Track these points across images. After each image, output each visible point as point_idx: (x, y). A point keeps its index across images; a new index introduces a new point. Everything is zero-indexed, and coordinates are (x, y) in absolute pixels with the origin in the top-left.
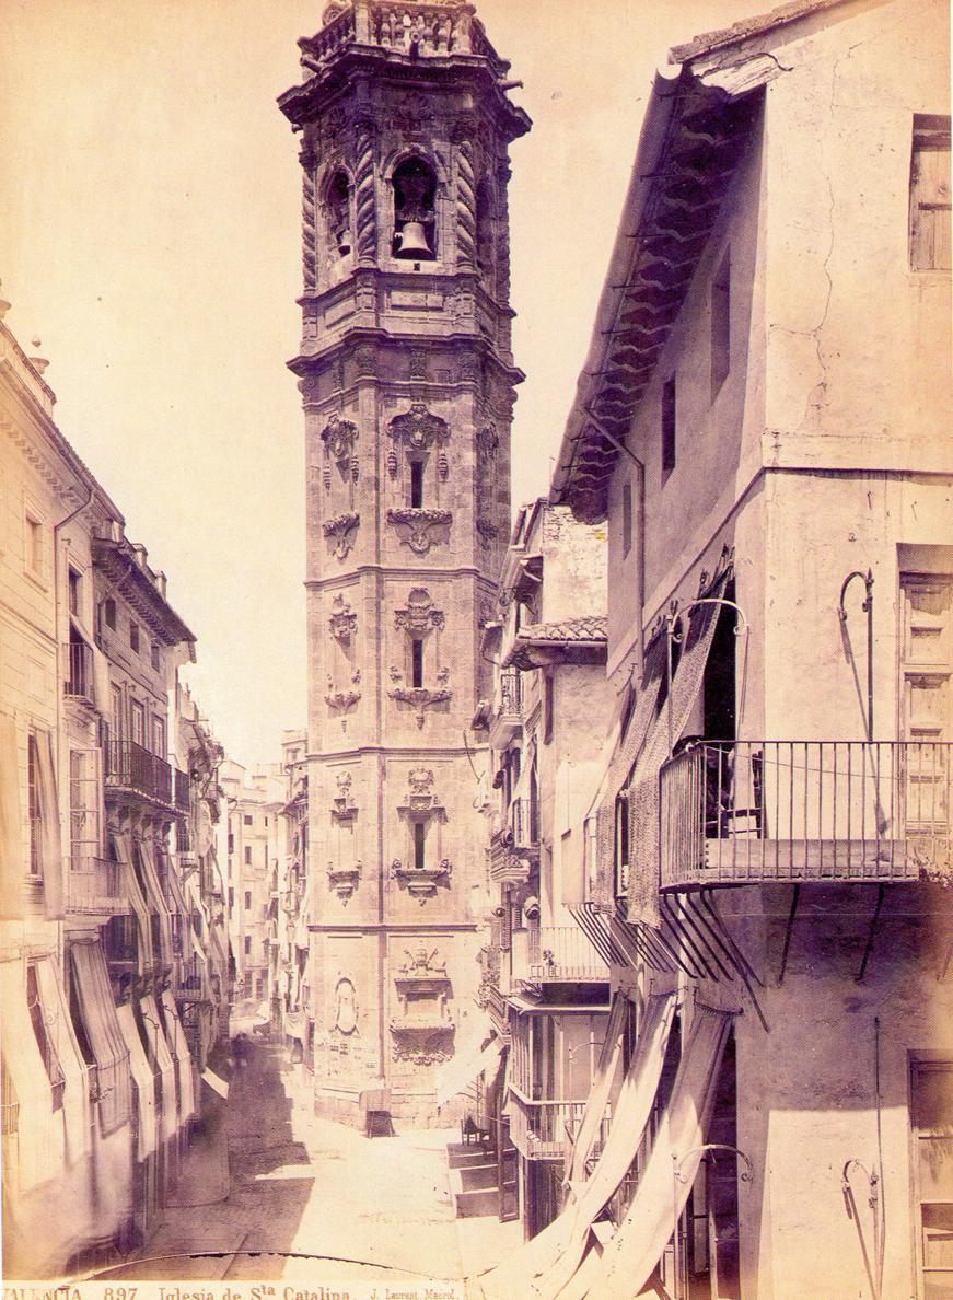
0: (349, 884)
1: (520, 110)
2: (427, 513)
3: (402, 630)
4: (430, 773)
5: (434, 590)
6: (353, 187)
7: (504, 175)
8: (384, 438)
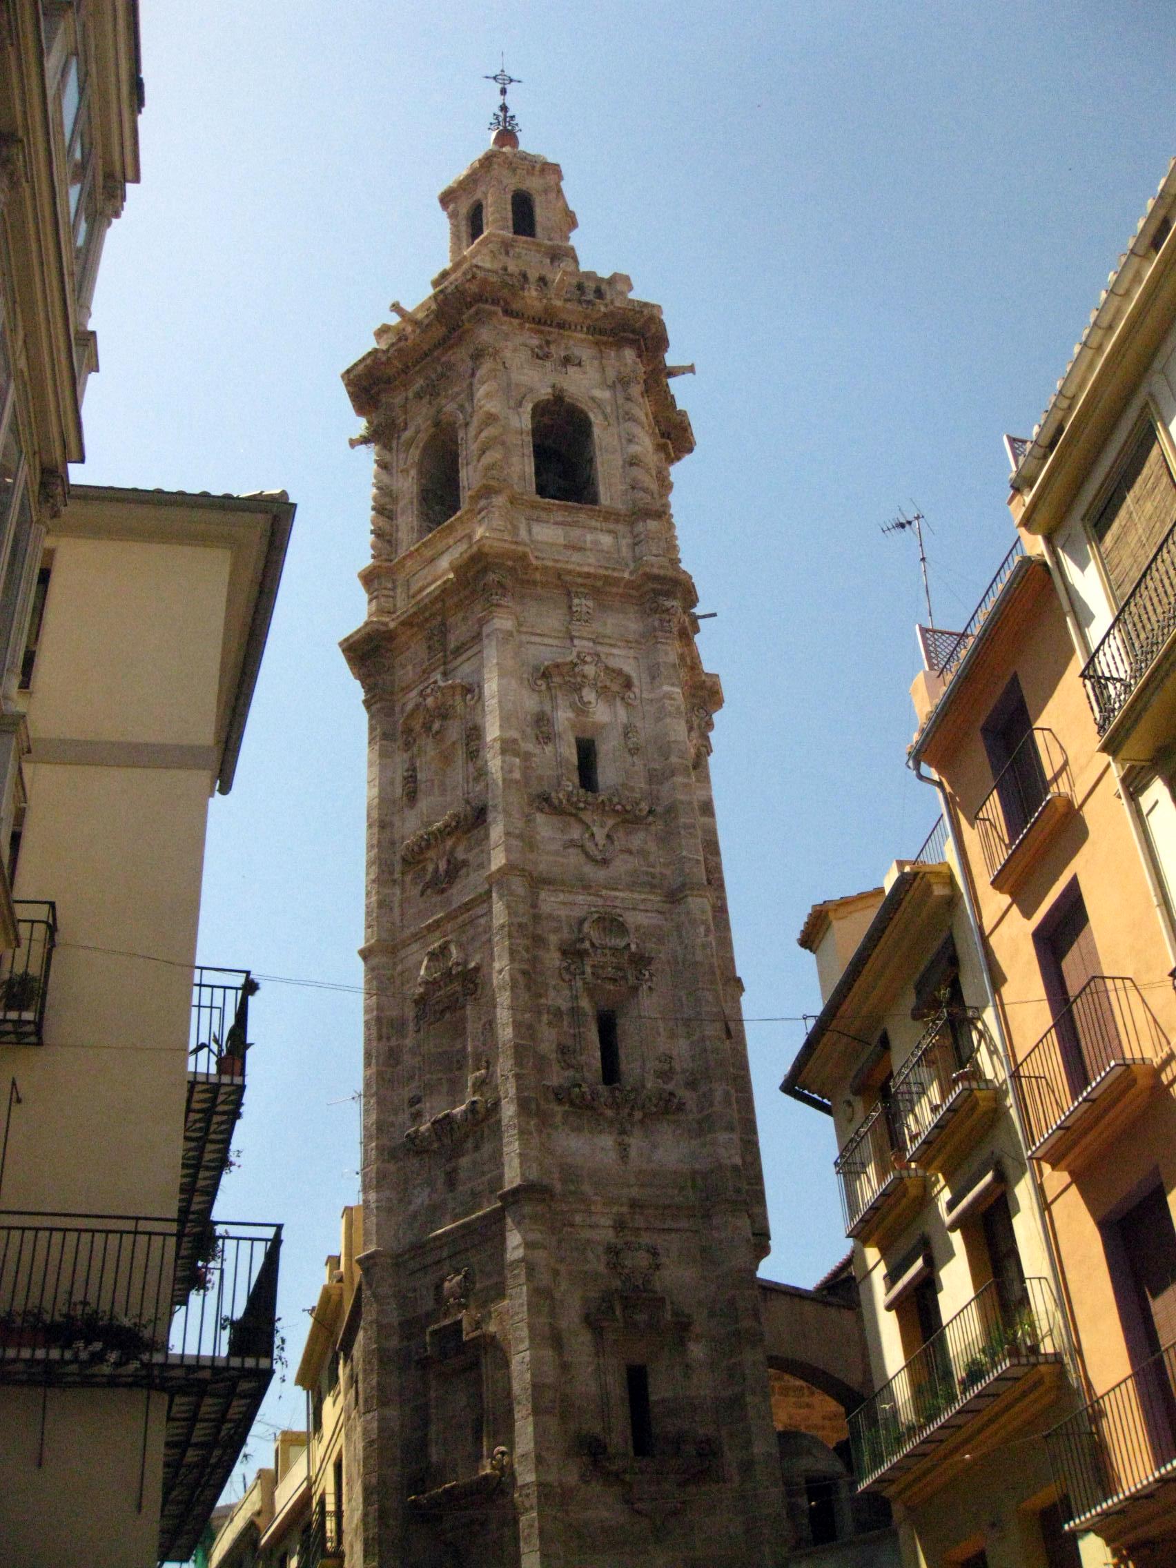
1: (683, 414)
4: (654, 1252)
5: (633, 919)
6: (467, 424)
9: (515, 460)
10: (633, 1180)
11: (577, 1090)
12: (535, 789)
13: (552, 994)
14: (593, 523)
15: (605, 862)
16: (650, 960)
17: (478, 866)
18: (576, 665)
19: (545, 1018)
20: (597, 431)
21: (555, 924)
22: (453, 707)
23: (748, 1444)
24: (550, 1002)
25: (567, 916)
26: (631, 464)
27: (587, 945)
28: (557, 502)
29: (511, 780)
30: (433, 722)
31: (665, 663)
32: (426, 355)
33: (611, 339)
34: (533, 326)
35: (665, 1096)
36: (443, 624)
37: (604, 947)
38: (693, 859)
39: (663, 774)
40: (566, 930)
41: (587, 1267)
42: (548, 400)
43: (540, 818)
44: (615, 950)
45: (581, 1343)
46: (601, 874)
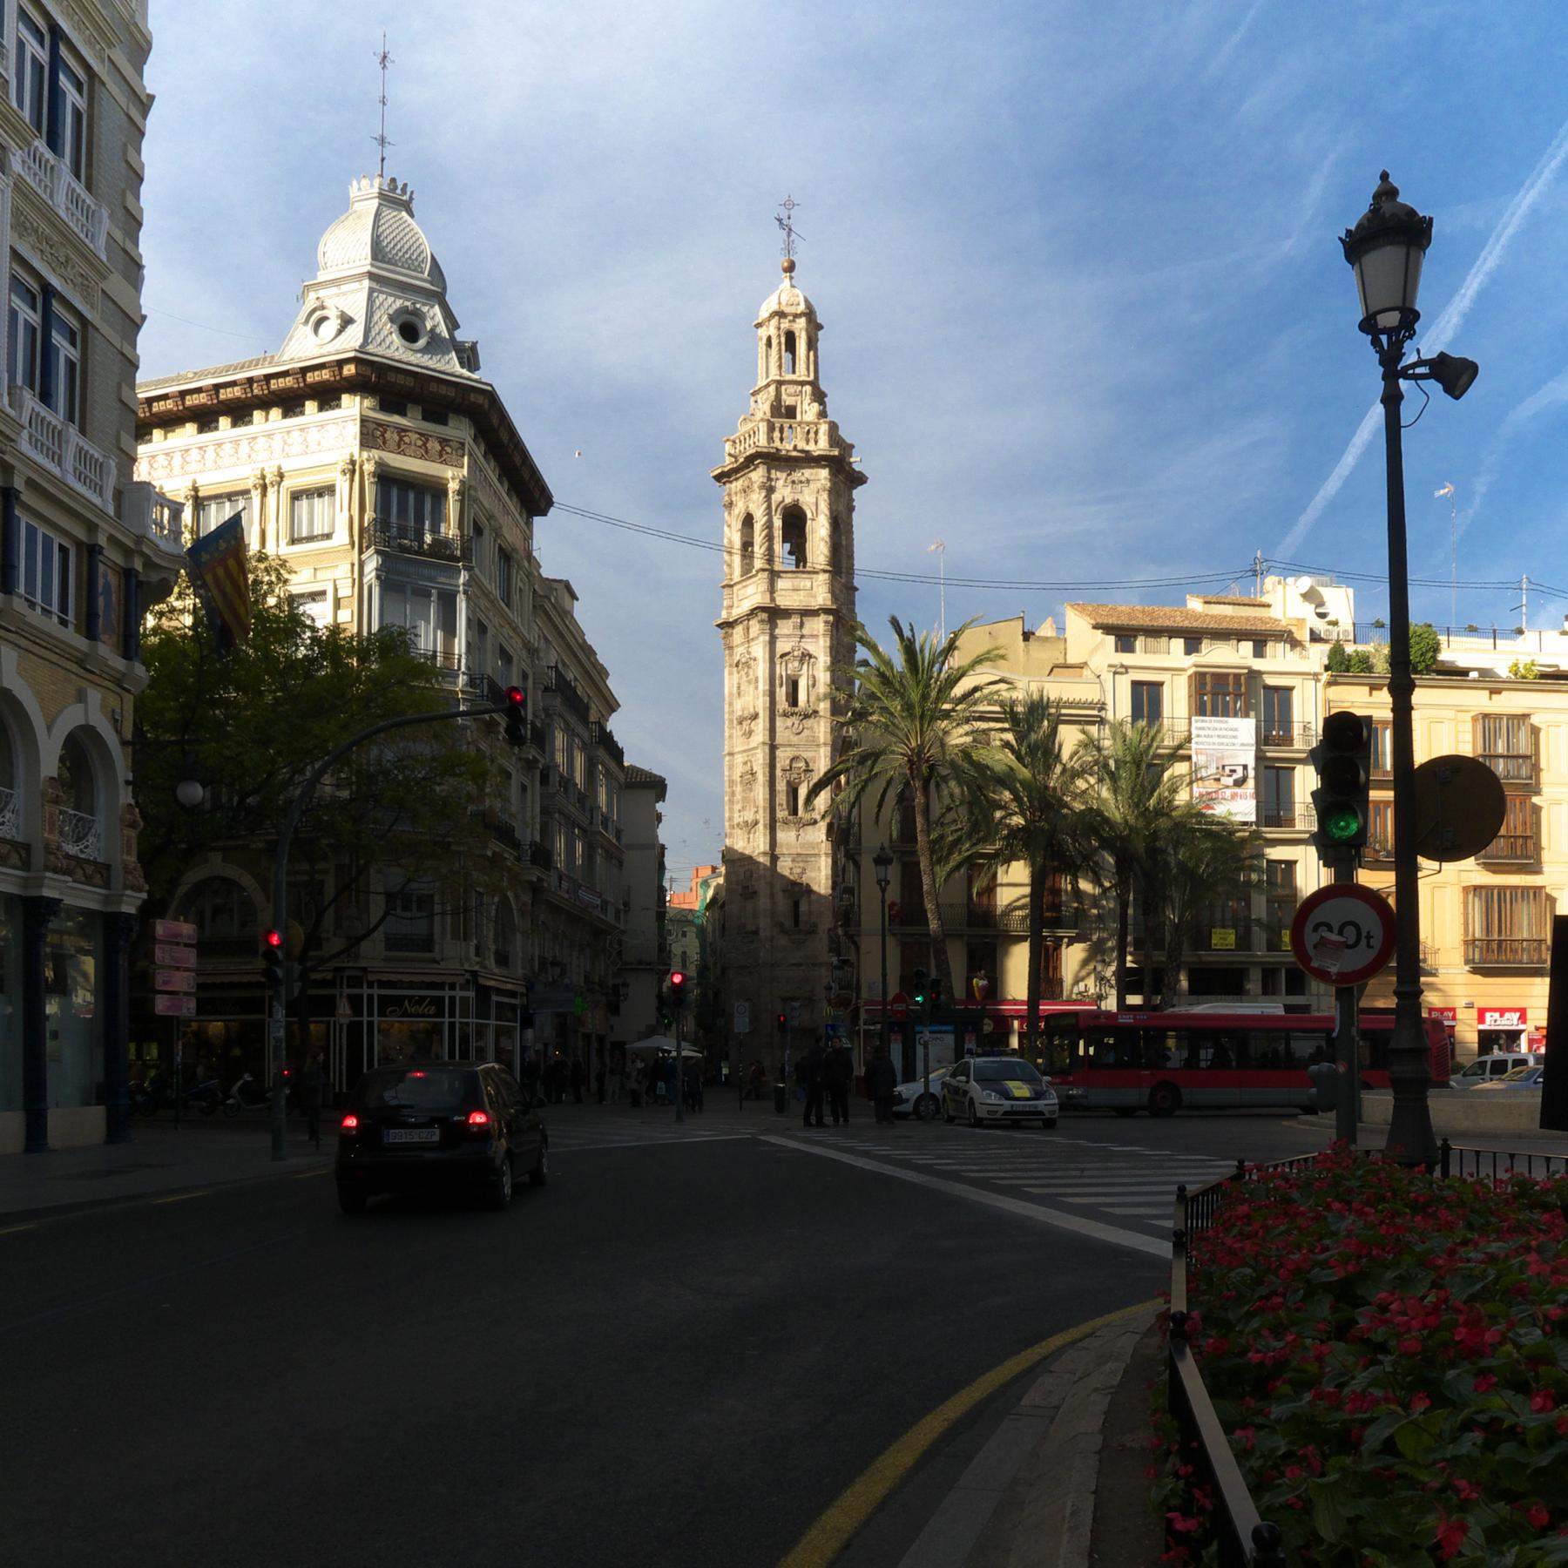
7: (851, 509)
20: (809, 522)
45: (780, 896)
46: (795, 739)
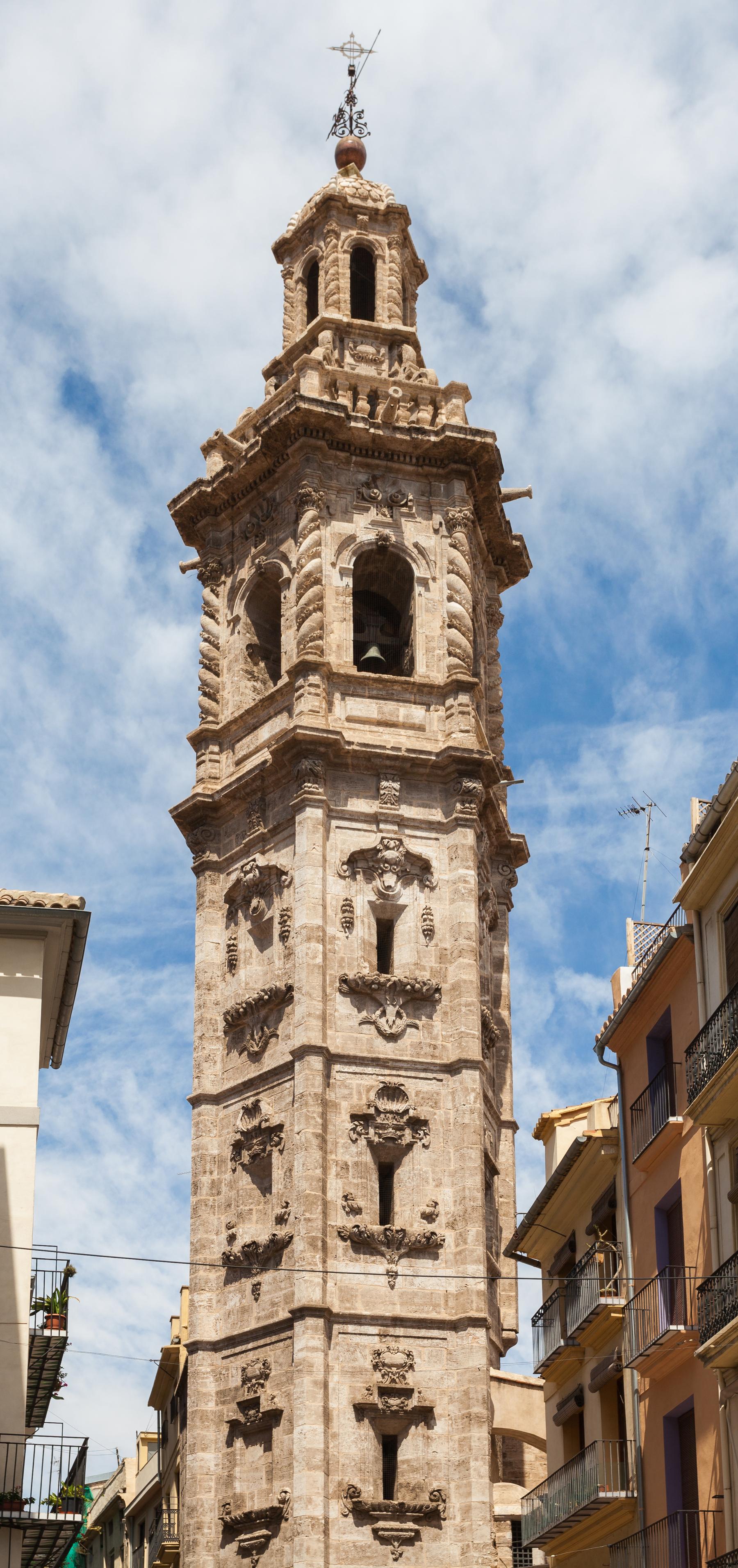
0: (264, 1532)
2: (405, 980)
3: (363, 1142)
4: (409, 1355)
5: (411, 1086)
8: (332, 879)
9: (336, 626)
10: (396, 1299)
11: (356, 1230)
12: (334, 972)
13: (340, 1150)
14: (407, 696)
15: (392, 1038)
16: (425, 1123)
17: (286, 1036)
18: (380, 851)
19: (333, 1170)
20: (418, 589)
21: (346, 1092)
22: (269, 885)
23: (469, 1494)
24: (339, 1158)
25: (357, 1084)
26: (450, 626)
27: (372, 1111)
28: (372, 675)
29: (315, 965)
30: (251, 898)
31: (463, 845)
32: (252, 488)
33: (441, 471)
34: (359, 459)
35: (428, 1234)
36: (263, 799)
37: (387, 1112)
38: (470, 1034)
39: (452, 953)
40: (355, 1097)
41: (356, 1364)
42: (372, 550)
43: (339, 997)
44: (396, 1113)
